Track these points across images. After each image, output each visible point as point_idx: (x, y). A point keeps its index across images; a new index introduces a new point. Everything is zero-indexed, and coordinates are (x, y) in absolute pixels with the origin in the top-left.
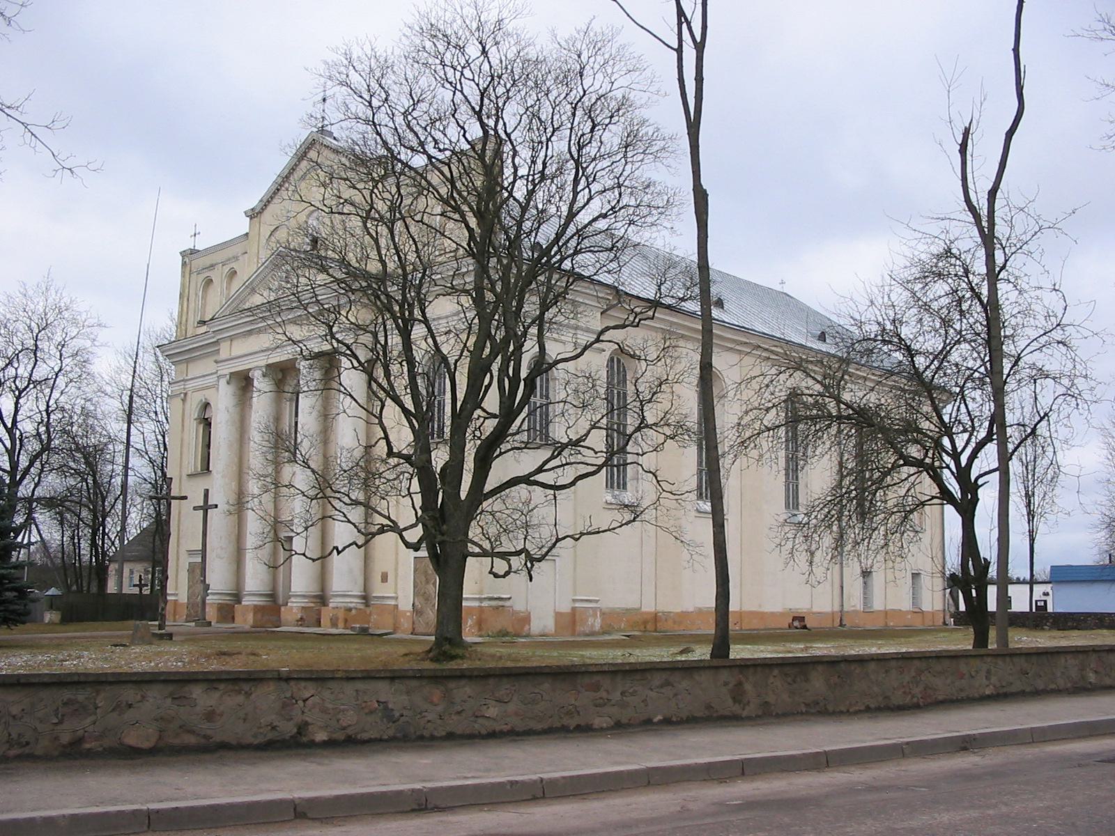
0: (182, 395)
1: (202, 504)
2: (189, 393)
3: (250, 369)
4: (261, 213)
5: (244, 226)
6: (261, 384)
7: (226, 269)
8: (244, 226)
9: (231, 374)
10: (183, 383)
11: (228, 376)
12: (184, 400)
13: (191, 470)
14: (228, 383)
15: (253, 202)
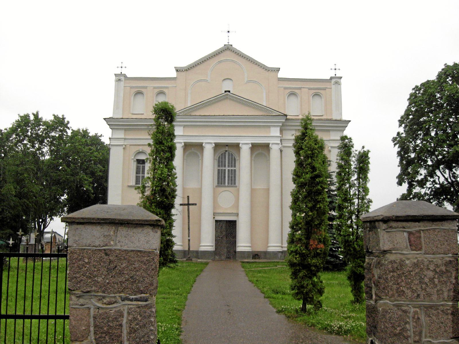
0: (124, 146)
1: (187, 203)
2: (128, 146)
3: (203, 143)
4: (186, 70)
5: (174, 74)
6: (208, 152)
7: (157, 90)
8: (174, 74)
9: (185, 143)
10: (123, 140)
11: (183, 144)
12: (124, 148)
13: (131, 184)
14: (182, 147)
15: (184, 63)
